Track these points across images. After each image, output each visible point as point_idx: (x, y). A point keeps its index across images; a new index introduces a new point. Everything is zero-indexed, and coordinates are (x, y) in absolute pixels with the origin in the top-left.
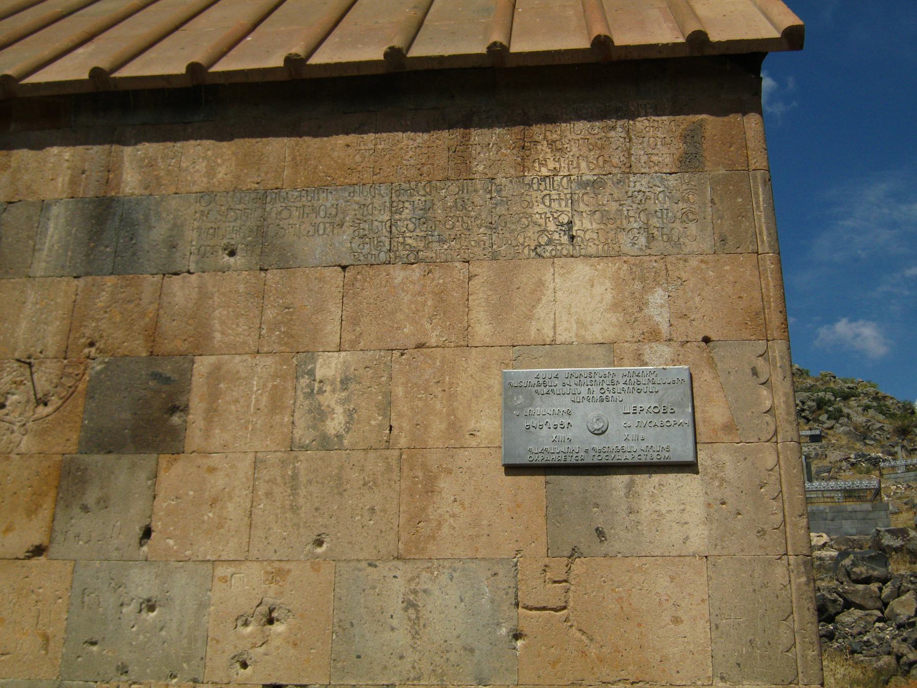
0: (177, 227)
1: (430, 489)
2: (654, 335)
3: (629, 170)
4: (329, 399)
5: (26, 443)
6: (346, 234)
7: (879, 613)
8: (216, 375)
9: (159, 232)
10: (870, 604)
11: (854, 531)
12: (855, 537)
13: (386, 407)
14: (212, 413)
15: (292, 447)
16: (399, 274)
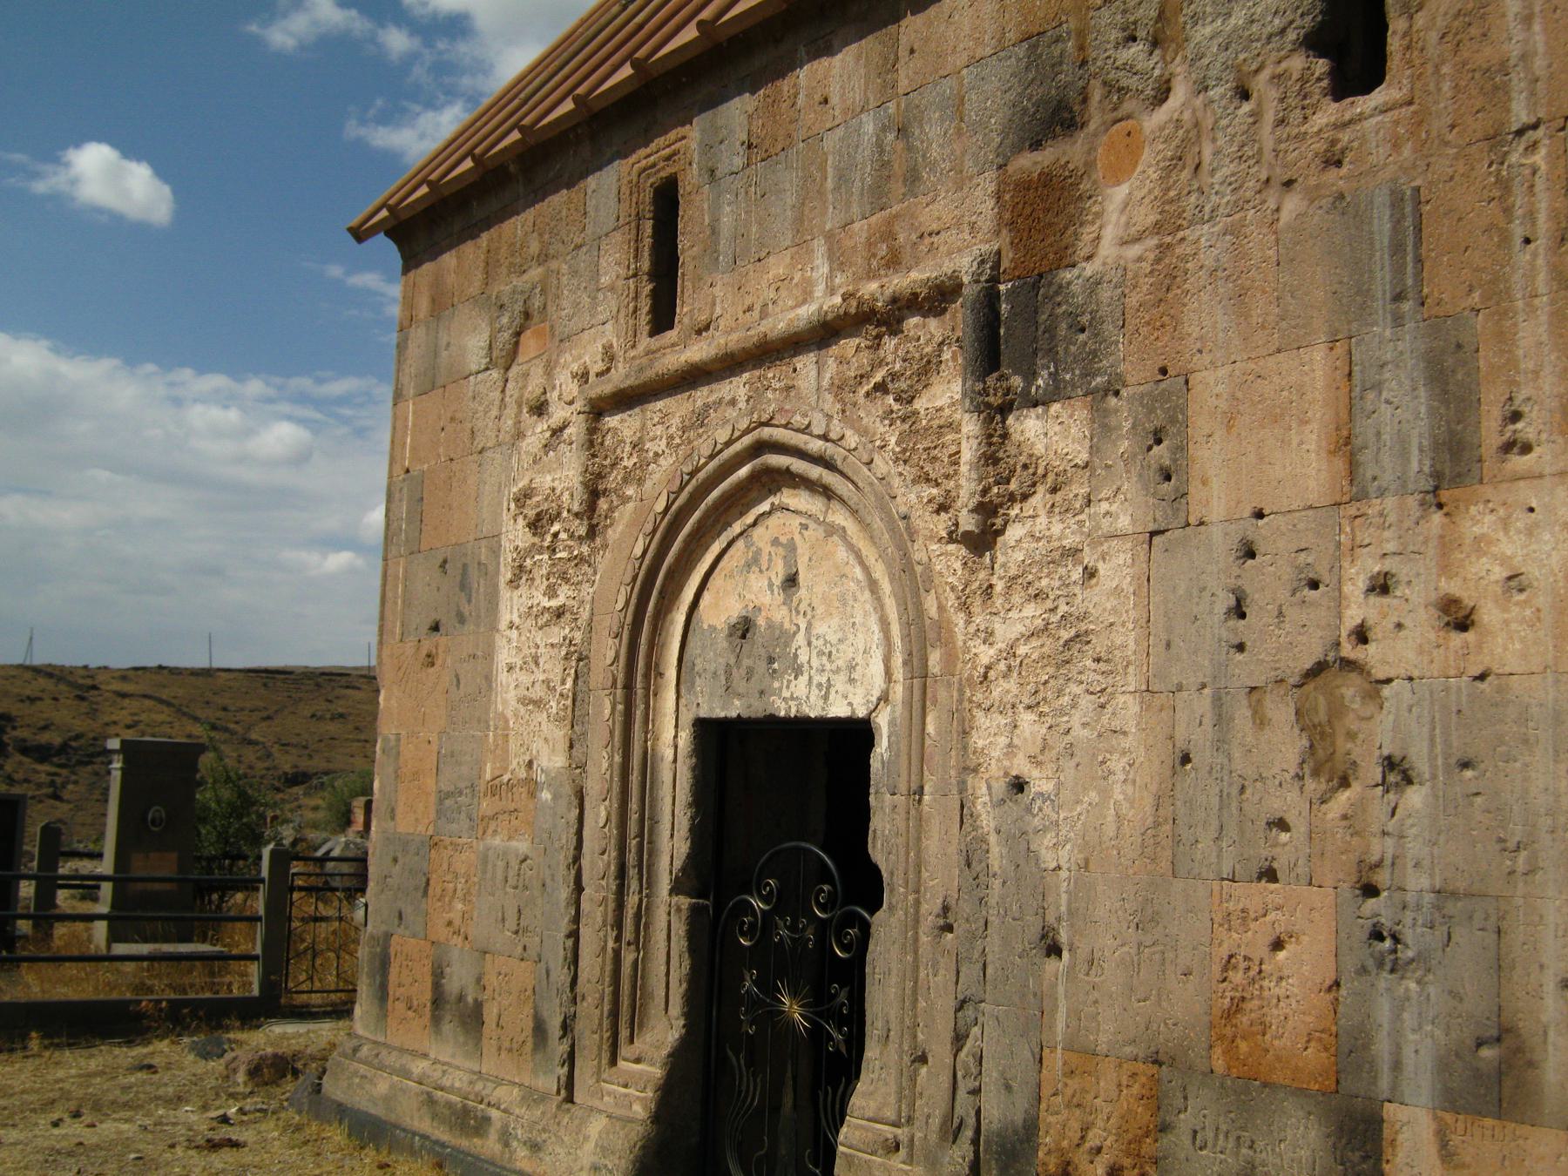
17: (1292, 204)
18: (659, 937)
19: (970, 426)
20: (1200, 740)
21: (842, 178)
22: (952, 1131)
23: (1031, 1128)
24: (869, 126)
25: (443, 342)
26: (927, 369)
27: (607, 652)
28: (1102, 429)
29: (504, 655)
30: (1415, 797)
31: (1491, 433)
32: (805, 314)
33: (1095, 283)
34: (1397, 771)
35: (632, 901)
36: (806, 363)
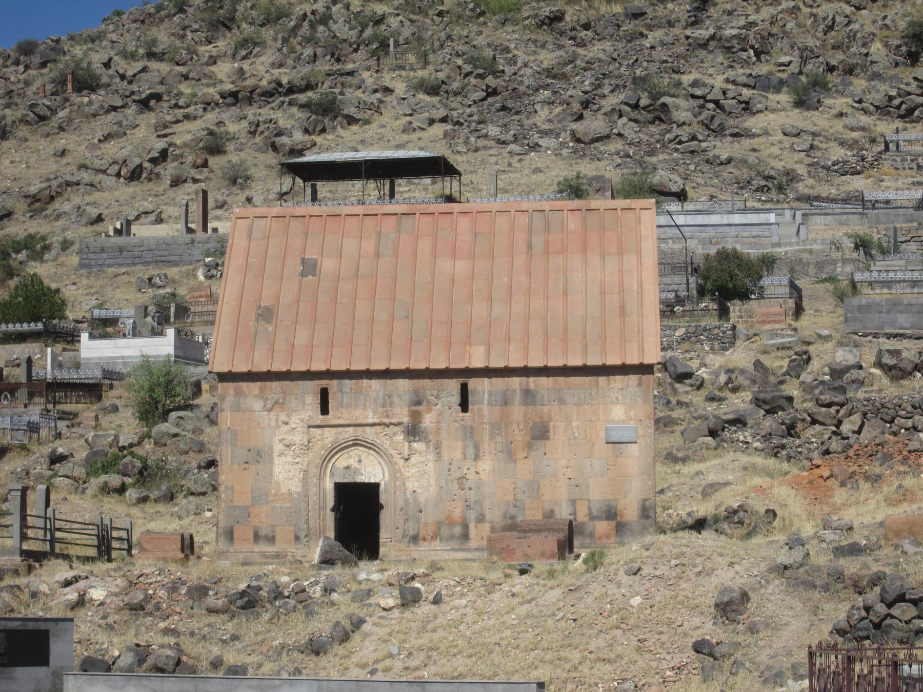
0: (543, 397)
1: (593, 446)
2: (631, 419)
3: (628, 386)
4: (575, 430)
5: (520, 439)
6: (576, 399)
7: (834, 428)
8: (554, 426)
9: (539, 397)
10: (828, 421)
11: (908, 325)
12: (909, 331)
13: (585, 432)
14: (554, 433)
15: (569, 439)
16: (586, 407)
17: (456, 424)
18: (328, 520)
19: (407, 444)
20: (444, 486)
21: (375, 400)
22: (403, 537)
23: (418, 534)
24: (381, 394)
25: (242, 401)
26: (395, 434)
27: (314, 470)
28: (428, 447)
29: (276, 470)
30: (472, 492)
31: (481, 454)
32: (370, 421)
33: (426, 428)
34: (470, 489)
35: (322, 513)
36: (368, 429)
